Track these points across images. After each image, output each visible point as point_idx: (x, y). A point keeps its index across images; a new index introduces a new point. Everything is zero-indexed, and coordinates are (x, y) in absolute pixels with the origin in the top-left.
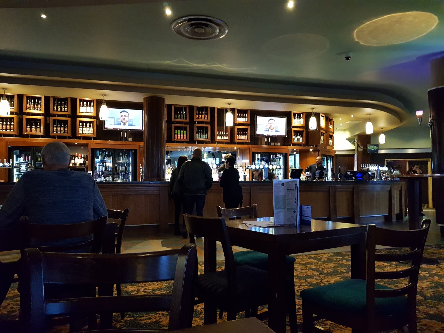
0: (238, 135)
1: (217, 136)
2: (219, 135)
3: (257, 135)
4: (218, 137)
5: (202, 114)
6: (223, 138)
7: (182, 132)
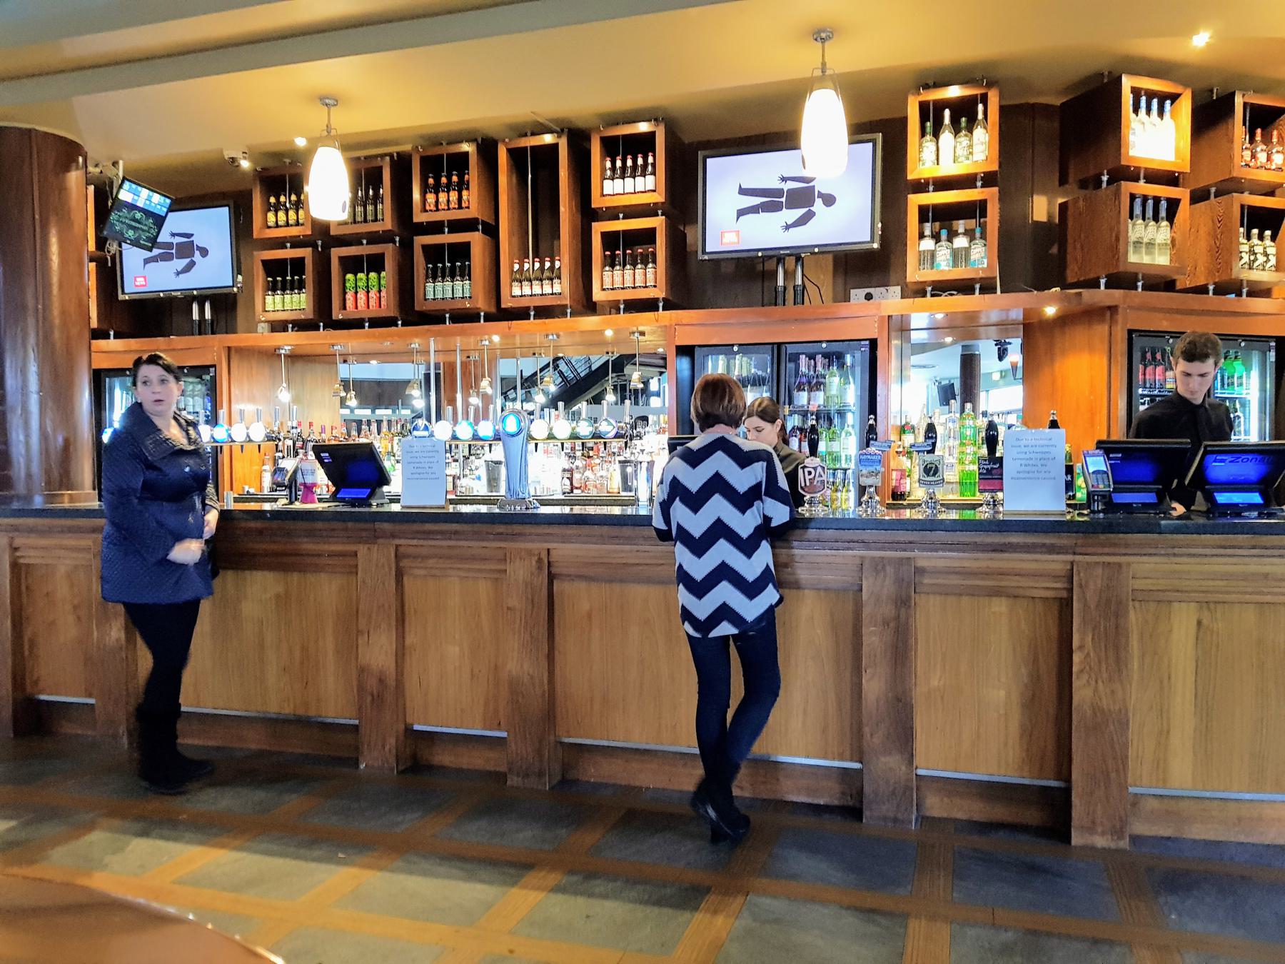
0: (607, 268)
1: (513, 281)
2: (521, 278)
3: (706, 257)
4: (513, 288)
5: (449, 187)
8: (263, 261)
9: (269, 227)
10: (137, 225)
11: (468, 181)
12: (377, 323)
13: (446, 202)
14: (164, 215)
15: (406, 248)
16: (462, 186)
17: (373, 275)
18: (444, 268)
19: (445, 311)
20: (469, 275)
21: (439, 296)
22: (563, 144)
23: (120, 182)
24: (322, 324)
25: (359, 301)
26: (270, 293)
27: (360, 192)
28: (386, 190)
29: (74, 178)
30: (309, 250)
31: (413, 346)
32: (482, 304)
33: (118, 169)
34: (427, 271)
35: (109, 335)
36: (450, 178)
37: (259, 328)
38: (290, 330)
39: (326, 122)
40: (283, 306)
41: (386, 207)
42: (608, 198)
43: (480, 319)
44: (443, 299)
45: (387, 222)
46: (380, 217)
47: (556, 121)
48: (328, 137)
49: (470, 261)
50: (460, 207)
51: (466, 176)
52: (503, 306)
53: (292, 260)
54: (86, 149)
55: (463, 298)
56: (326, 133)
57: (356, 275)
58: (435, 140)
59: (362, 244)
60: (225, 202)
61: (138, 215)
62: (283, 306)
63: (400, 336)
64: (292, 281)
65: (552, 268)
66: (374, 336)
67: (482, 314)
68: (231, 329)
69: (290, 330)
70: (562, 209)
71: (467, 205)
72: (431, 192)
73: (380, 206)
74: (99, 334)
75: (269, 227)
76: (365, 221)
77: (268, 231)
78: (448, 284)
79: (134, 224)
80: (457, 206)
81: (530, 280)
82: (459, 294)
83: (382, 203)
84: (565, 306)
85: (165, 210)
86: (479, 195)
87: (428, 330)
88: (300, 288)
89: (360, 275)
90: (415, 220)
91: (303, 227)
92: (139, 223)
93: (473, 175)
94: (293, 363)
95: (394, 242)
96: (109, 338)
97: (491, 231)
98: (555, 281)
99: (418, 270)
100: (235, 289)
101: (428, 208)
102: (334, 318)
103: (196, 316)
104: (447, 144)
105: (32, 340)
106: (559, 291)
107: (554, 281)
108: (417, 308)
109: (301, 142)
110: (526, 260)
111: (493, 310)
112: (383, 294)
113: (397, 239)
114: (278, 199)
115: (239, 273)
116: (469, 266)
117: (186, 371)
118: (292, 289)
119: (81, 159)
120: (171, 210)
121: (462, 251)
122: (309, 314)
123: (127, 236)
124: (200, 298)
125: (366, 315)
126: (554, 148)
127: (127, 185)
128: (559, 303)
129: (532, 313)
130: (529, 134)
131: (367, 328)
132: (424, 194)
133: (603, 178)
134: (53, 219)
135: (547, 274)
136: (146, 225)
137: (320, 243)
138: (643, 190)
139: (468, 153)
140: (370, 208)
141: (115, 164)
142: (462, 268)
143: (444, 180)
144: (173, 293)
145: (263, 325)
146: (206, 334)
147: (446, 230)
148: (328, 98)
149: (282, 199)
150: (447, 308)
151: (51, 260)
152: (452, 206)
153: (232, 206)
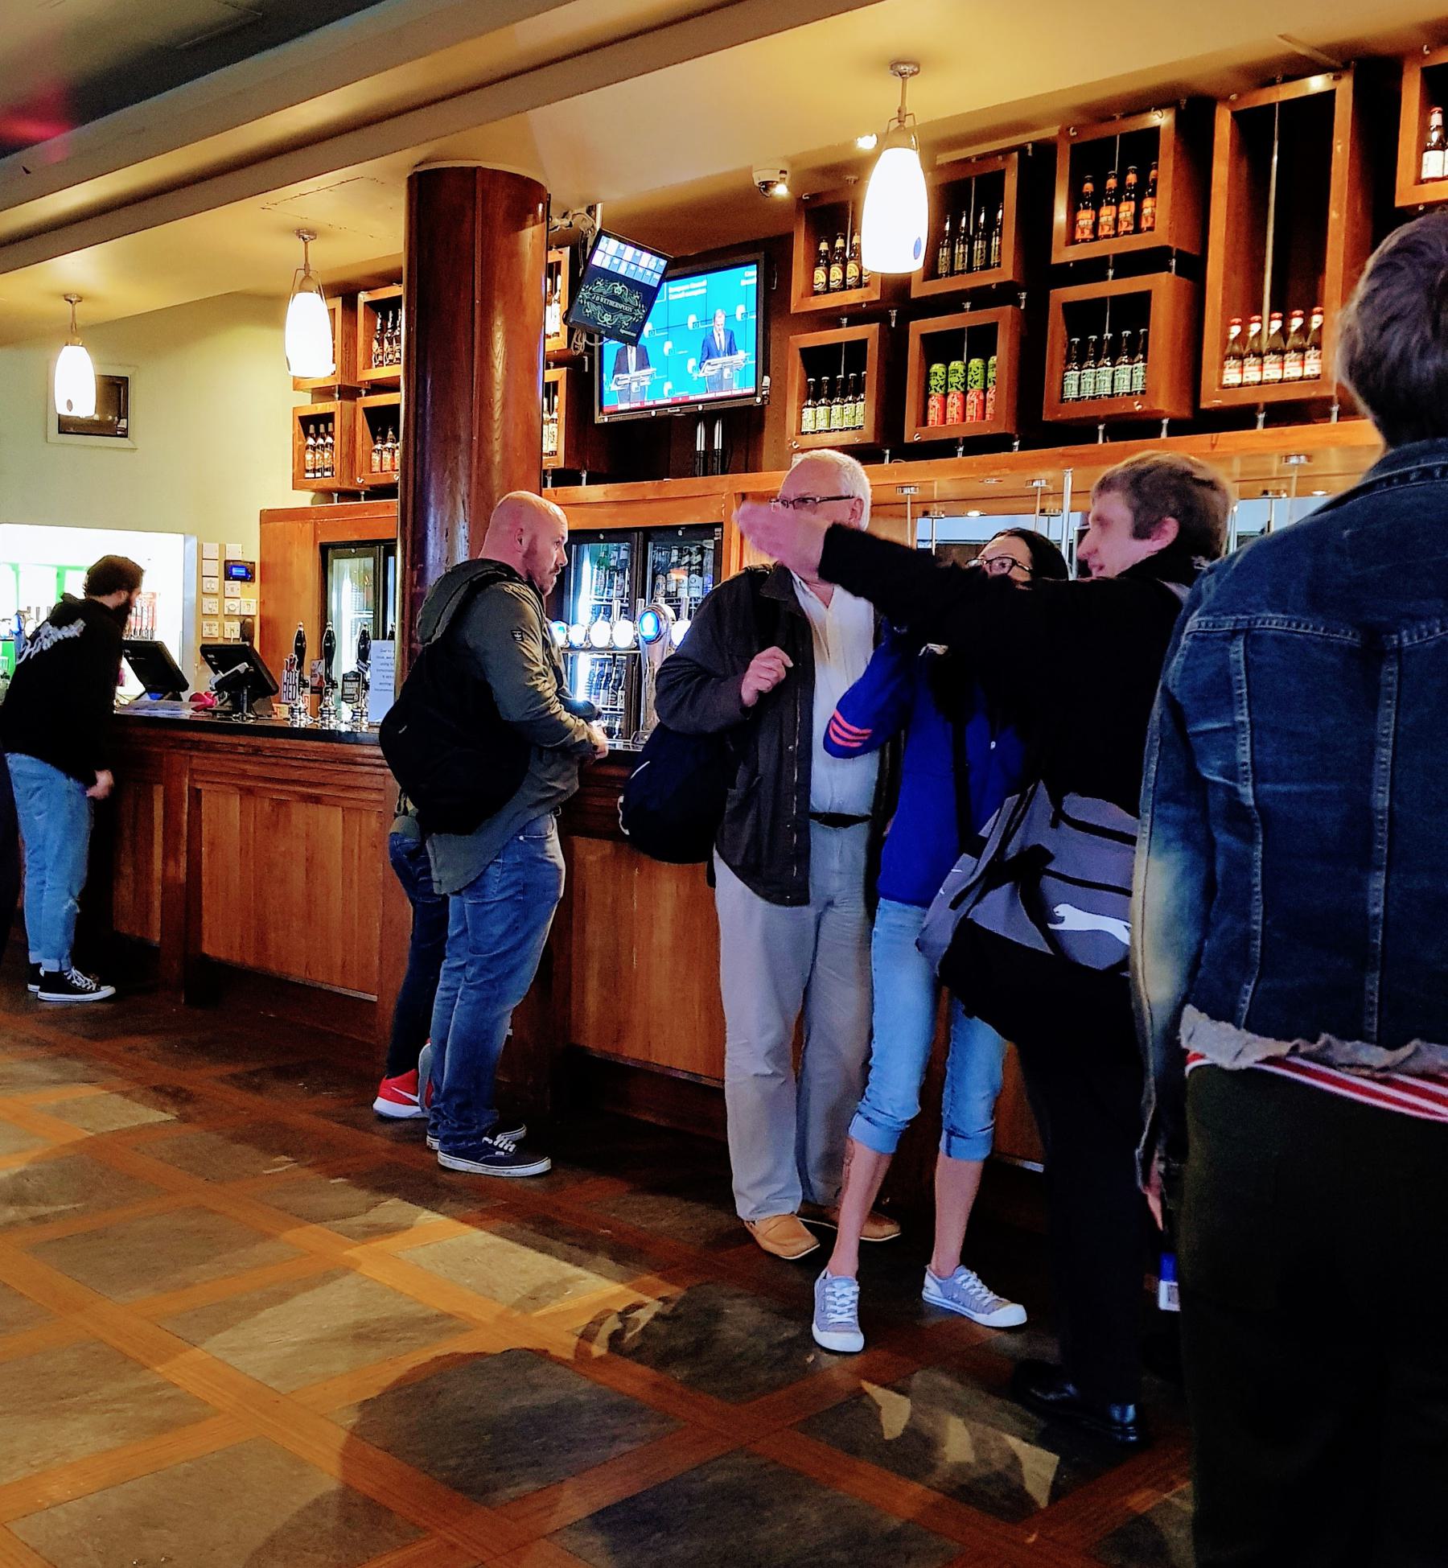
1: (1227, 358)
2: (1244, 350)
4: (1227, 371)
5: (1117, 198)
6: (1272, 370)
9: (817, 293)
10: (618, 305)
11: (1155, 181)
12: (978, 445)
13: (1111, 223)
16: (1145, 189)
17: (976, 363)
18: (1100, 341)
19: (1097, 420)
20: (1145, 352)
21: (1088, 392)
22: (1345, 89)
24: (888, 452)
25: (949, 409)
28: (1007, 213)
29: (531, 236)
30: (876, 325)
32: (1165, 404)
34: (1069, 350)
36: (1121, 179)
39: (899, 105)
41: (1005, 244)
42: (1430, 185)
43: (1161, 431)
44: (1094, 398)
45: (1006, 271)
46: (994, 260)
47: (1330, 50)
48: (894, 134)
49: (1147, 327)
50: (1138, 229)
51: (1153, 172)
52: (1204, 405)
53: (849, 344)
55: (1130, 394)
56: (896, 124)
57: (947, 365)
58: (1100, 112)
59: (964, 310)
60: (751, 257)
64: (846, 380)
65: (1304, 330)
66: (969, 468)
67: (1165, 421)
68: (752, 466)
70: (1333, 215)
71: (1149, 225)
72: (1086, 208)
73: (995, 242)
74: (565, 478)
75: (817, 293)
77: (812, 299)
78: (1106, 372)
79: (612, 303)
80: (1131, 228)
81: (1259, 355)
82: (1123, 387)
83: (1000, 236)
84: (1329, 401)
85: (658, 277)
86: (1174, 205)
87: (1063, 455)
88: (856, 395)
89: (956, 365)
92: (621, 302)
93: (1165, 170)
95: (1017, 303)
96: (580, 484)
97: (1193, 268)
98: (1312, 353)
99: (1053, 347)
101: (1079, 236)
102: (906, 440)
103: (700, 446)
104: (1123, 117)
105: (463, 488)
106: (1317, 372)
107: (1308, 353)
110: (1257, 318)
111: (1186, 413)
114: (832, 244)
115: (766, 372)
116: (1146, 334)
117: (680, 533)
118: (844, 396)
120: (665, 278)
121: (1136, 308)
122: (868, 436)
123: (601, 323)
124: (709, 414)
126: (1328, 97)
128: (1313, 394)
129: (1261, 416)
130: (1279, 78)
131: (960, 455)
132: (1073, 211)
133: (1423, 148)
134: (499, 305)
135: (1294, 341)
137: (894, 313)
138: (1440, 175)
139: (1158, 128)
140: (979, 245)
141: (591, 210)
142: (1135, 337)
143: (1112, 183)
144: (669, 410)
147: (1111, 273)
148: (905, 63)
149: (839, 243)
150: (1102, 414)
151: (493, 366)
152: (1123, 228)
153: (762, 263)
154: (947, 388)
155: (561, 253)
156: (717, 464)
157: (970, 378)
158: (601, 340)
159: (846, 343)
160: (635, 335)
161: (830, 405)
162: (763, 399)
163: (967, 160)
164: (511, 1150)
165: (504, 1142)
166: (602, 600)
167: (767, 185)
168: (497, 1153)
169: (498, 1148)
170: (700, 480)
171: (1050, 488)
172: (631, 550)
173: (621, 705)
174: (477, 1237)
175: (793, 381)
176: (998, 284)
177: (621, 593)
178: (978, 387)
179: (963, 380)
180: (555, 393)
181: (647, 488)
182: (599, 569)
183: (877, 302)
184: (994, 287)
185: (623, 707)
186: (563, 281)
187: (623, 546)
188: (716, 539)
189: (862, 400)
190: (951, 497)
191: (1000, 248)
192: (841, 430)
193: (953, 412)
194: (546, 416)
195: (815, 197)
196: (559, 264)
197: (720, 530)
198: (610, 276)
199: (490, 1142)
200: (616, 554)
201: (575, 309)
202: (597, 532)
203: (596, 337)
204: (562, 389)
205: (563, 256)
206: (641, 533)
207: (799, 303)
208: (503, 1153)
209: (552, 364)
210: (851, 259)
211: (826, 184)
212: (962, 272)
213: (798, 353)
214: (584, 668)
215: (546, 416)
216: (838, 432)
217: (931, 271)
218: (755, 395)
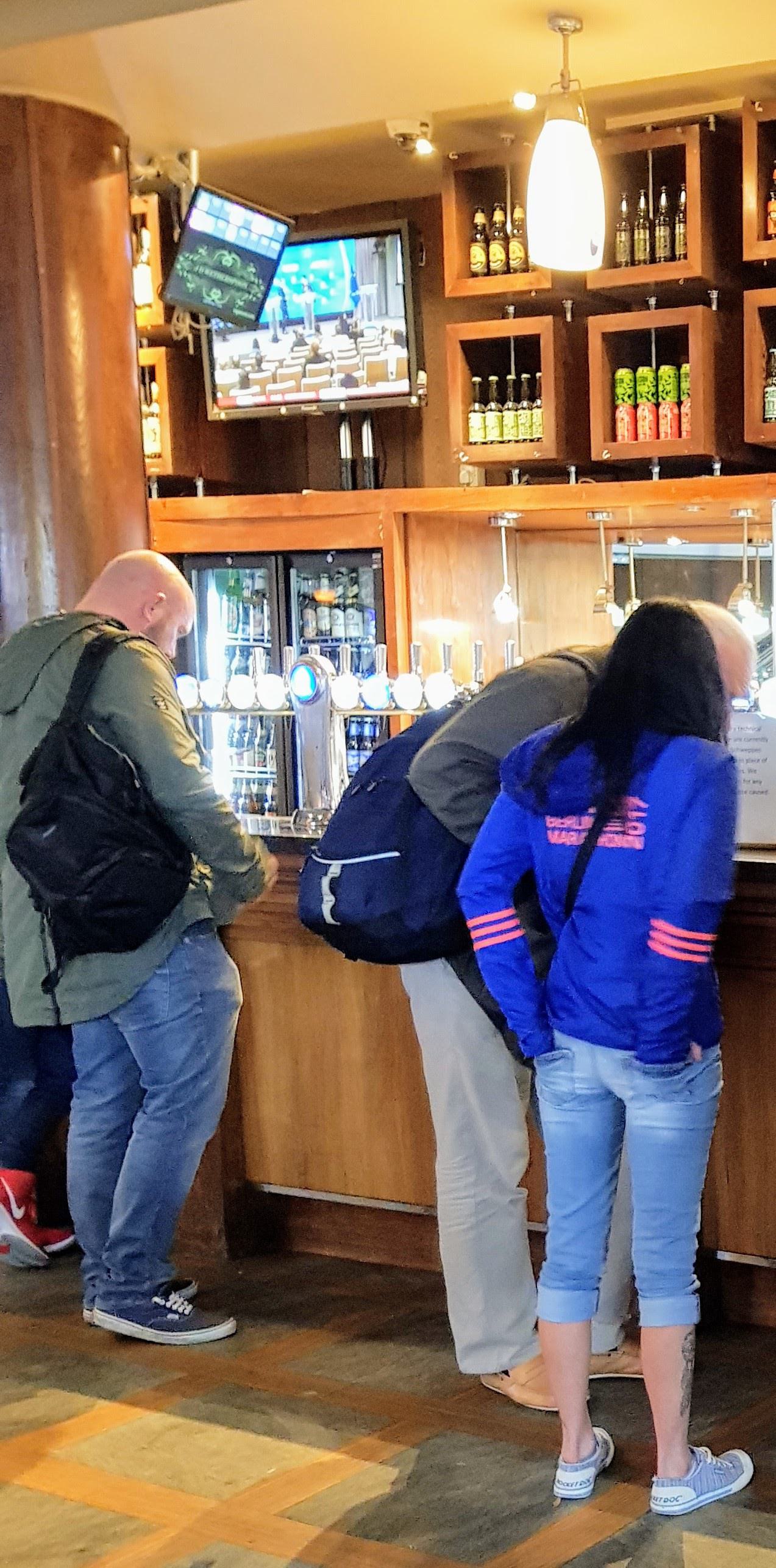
7: (645, 379)
8: (462, 342)
9: (475, 275)
10: (228, 279)
14: (275, 256)
15: (732, 307)
17: (666, 370)
23: (193, 190)
24: (573, 469)
25: (640, 423)
26: (477, 406)
27: (643, 200)
28: (692, 195)
30: (549, 319)
31: (742, 514)
33: (188, 167)
35: (196, 488)
37: (462, 473)
38: (515, 480)
40: (502, 435)
46: (679, 251)
54: (128, 131)
57: (635, 371)
61: (228, 259)
62: (502, 435)
63: (715, 493)
64: (518, 382)
68: (412, 480)
69: (515, 480)
73: (680, 229)
75: (475, 275)
76: (653, 260)
77: (471, 281)
79: (220, 276)
83: (685, 222)
85: (277, 247)
88: (532, 398)
89: (643, 371)
90: (748, 256)
91: (534, 274)
94: (525, 542)
96: (194, 494)
100: (414, 400)
102: (594, 457)
108: (748, 439)
109: (524, 102)
112: (685, 409)
113: (714, 295)
115: (421, 367)
117: (330, 559)
119: (117, 151)
120: (288, 243)
122: (548, 450)
123: (207, 300)
125: (654, 453)
127: (204, 199)
136: (242, 278)
137: (568, 304)
140: (661, 232)
141: (183, 157)
145: (470, 468)
146: (364, 488)
149: (498, 216)
154: (636, 398)
155: (146, 202)
156: (369, 476)
157: (661, 388)
158: (208, 321)
159: (516, 338)
160: (252, 317)
161: (501, 411)
162: (420, 397)
163: (641, 129)
164: (187, 1312)
165: (178, 1302)
166: (237, 639)
167: (406, 138)
168: (170, 1316)
169: (170, 1310)
170: (350, 494)
171: (757, 518)
172: (267, 578)
173: (272, 767)
174: (154, 1420)
175: (454, 381)
176: (686, 280)
177: (259, 630)
178: (671, 399)
179: (653, 390)
180: (153, 378)
181: (282, 502)
182: (229, 600)
183: (548, 290)
184: (681, 282)
185: (275, 770)
186: (150, 237)
187: (259, 572)
188: (375, 566)
189: (538, 407)
190: (648, 523)
191: (685, 236)
192: (517, 442)
193: (645, 427)
194: (144, 408)
195: (464, 157)
196: (143, 216)
197: (379, 556)
198: (217, 244)
199: (161, 1302)
200: (248, 582)
201: (172, 281)
202: (226, 555)
203: (202, 318)
204: (162, 374)
205: (149, 206)
206: (280, 558)
207: (453, 285)
208: (177, 1317)
209: (145, 342)
210: (514, 236)
211: (475, 143)
212: (645, 262)
213: (459, 346)
214: (222, 726)
215: (144, 408)
216: (512, 444)
217: (611, 262)
218: (410, 394)
